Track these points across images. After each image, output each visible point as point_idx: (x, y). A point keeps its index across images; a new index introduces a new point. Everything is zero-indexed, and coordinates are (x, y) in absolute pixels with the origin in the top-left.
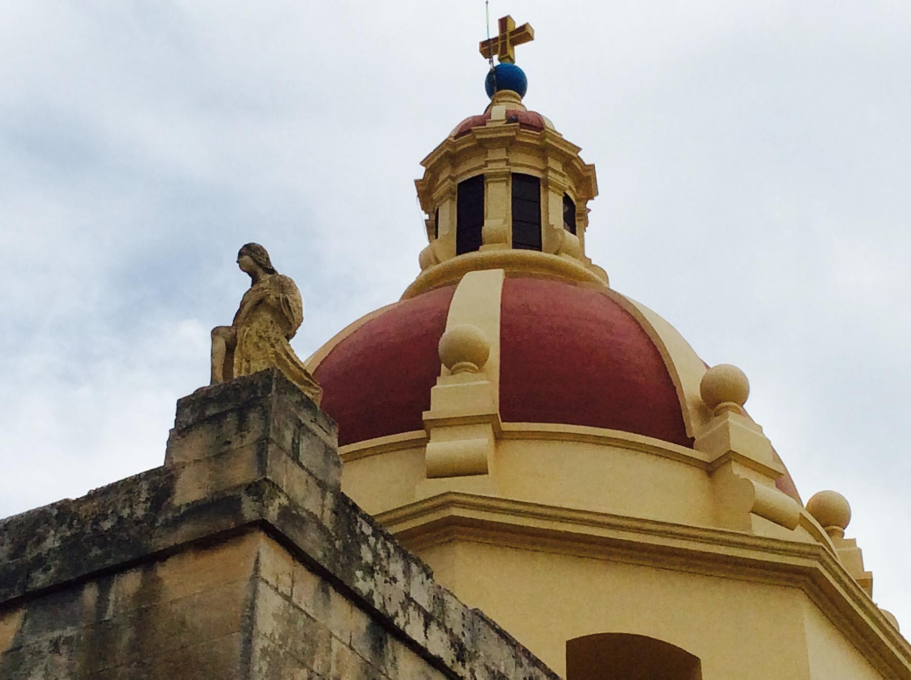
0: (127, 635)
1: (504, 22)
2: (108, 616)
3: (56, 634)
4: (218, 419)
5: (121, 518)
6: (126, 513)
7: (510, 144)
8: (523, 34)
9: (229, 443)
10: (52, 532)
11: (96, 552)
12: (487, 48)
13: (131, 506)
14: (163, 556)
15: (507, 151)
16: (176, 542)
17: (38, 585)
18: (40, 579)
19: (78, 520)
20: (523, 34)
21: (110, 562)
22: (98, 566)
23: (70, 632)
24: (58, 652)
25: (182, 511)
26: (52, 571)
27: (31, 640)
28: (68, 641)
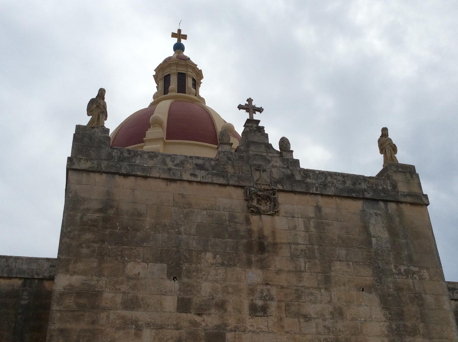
0: (397, 219)
1: (179, 31)
2: (390, 212)
3: (375, 211)
4: (405, 173)
5: (384, 188)
6: (385, 187)
7: (177, 65)
8: (185, 37)
9: (410, 180)
10: (363, 183)
11: (382, 194)
12: (174, 35)
13: (386, 185)
14: (402, 203)
15: (177, 67)
16: (407, 201)
17: (368, 196)
18: (368, 196)
19: (371, 183)
20: (185, 37)
21: (388, 199)
22: (385, 199)
23: (379, 212)
24: (377, 216)
25: (406, 193)
26: (370, 194)
27: (367, 210)
28: (380, 214)
